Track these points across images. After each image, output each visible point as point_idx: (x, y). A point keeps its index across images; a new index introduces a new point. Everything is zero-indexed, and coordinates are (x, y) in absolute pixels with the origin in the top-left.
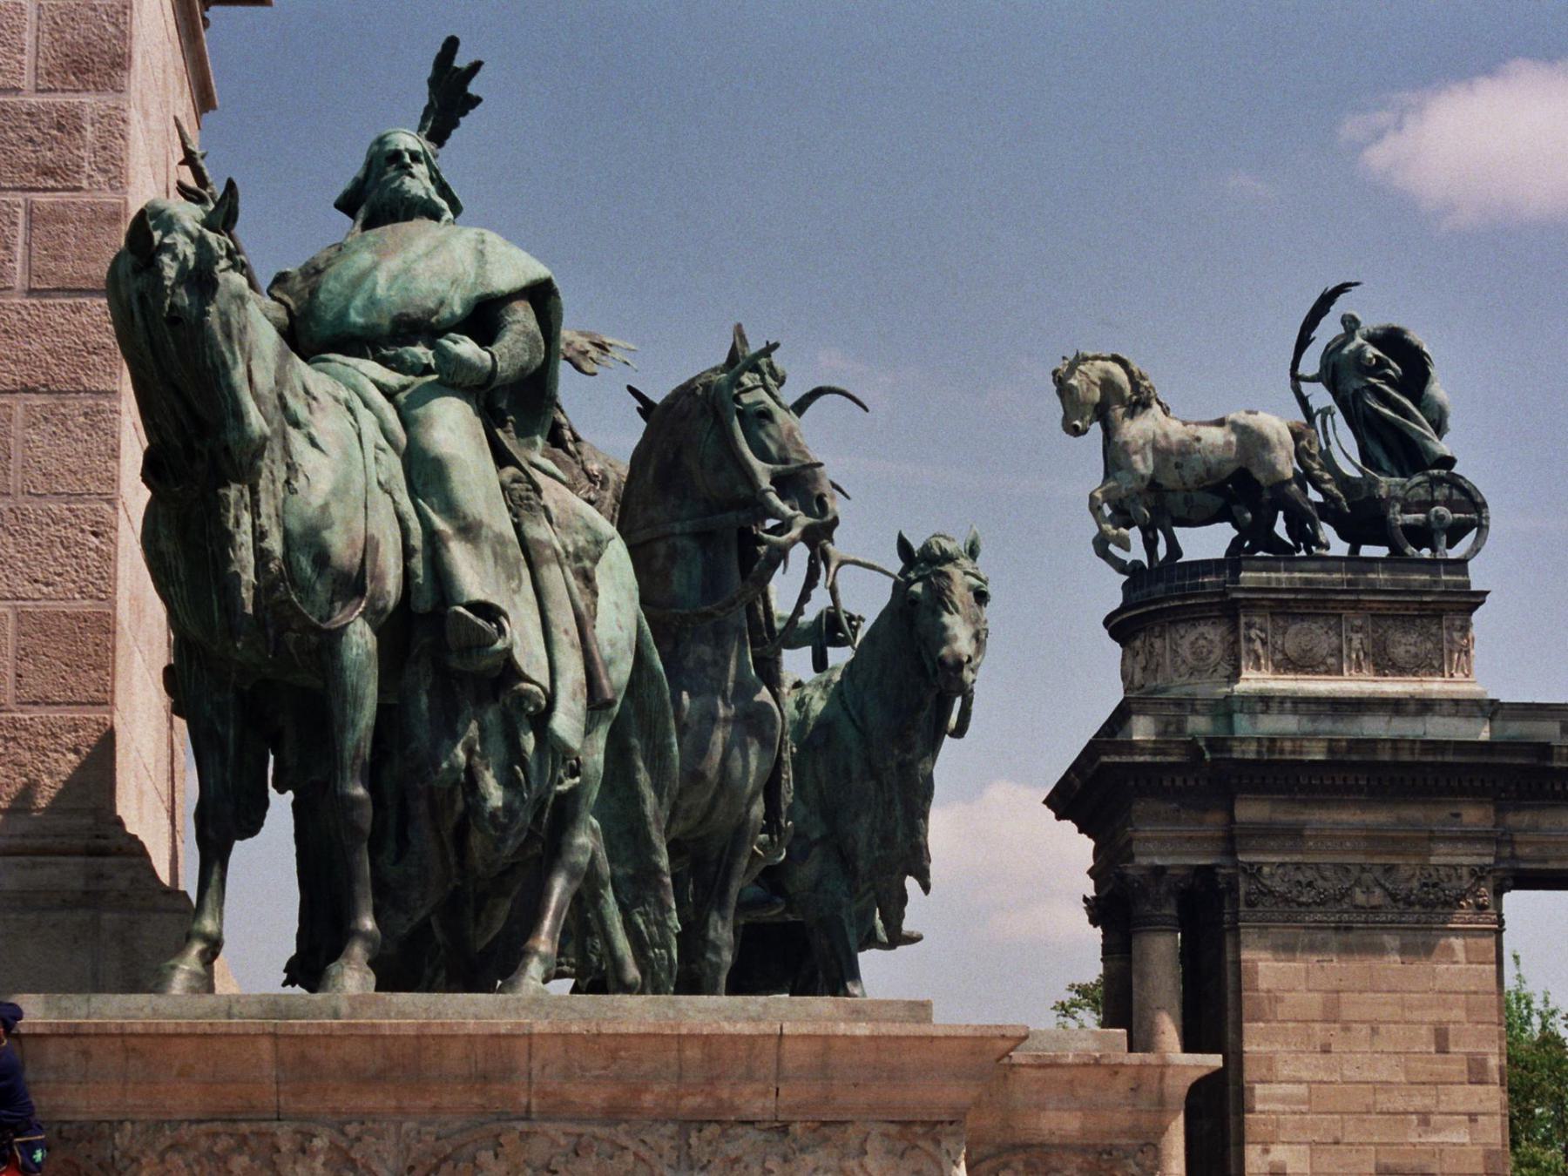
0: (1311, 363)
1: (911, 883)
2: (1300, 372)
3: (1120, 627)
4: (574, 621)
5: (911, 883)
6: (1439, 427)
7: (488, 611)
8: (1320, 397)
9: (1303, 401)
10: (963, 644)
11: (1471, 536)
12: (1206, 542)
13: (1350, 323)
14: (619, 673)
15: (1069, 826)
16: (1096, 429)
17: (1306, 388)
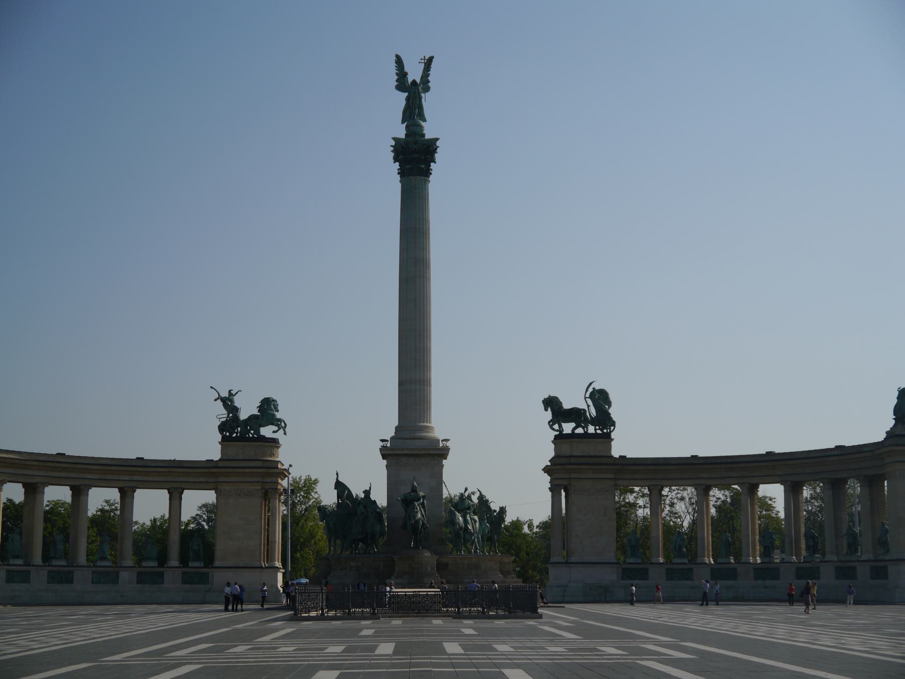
0: (588, 395)
3: (553, 442)
6: (610, 406)
8: (589, 401)
12: (568, 427)
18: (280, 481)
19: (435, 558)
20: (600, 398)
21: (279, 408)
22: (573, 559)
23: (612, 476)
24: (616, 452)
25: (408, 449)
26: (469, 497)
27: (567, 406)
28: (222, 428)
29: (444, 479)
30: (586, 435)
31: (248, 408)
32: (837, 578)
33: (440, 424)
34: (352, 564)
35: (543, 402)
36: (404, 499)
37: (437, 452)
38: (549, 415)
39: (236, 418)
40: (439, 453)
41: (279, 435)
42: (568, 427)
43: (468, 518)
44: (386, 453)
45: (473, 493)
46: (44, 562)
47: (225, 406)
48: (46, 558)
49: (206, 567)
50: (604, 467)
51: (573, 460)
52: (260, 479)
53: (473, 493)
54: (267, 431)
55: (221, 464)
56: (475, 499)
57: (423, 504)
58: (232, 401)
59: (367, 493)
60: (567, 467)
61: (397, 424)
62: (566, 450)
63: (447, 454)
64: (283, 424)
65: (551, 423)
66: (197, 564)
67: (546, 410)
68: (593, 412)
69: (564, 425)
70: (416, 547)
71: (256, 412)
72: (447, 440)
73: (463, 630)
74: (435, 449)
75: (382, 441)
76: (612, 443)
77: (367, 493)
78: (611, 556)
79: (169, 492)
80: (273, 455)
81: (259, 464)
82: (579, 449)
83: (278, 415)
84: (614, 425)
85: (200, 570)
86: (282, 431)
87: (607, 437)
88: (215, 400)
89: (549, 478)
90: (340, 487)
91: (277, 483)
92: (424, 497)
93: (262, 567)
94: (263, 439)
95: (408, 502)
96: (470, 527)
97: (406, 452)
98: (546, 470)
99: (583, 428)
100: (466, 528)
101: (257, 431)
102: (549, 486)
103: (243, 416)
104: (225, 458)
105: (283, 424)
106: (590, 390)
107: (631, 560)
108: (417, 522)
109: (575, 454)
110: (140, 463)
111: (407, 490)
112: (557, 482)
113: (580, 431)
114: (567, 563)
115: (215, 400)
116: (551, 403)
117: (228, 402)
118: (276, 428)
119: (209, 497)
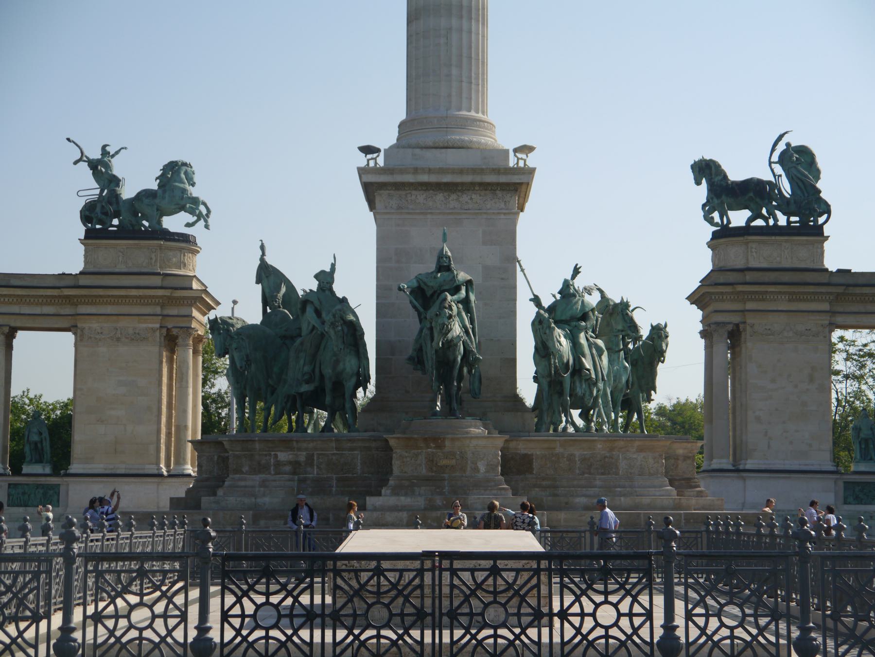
0: (775, 158)
1: (653, 392)
2: (772, 160)
3: (710, 245)
4: (599, 362)
5: (653, 392)
6: (818, 178)
7: (588, 370)
8: (778, 169)
9: (772, 170)
10: (664, 348)
11: (826, 216)
12: (739, 218)
13: (788, 145)
14: (605, 373)
15: (694, 307)
16: (704, 181)
17: (773, 165)
18: (195, 313)
19: (499, 441)
20: (799, 162)
21: (196, 179)
22: (750, 464)
23: (825, 306)
24: (833, 261)
25: (430, 171)
27: (736, 173)
28: (88, 214)
29: (520, 254)
30: (776, 230)
31: (136, 178)
33: (508, 115)
34: (283, 456)
35: (693, 167)
36: (422, 294)
37: (503, 179)
38: (702, 192)
40: (505, 186)
41: (197, 231)
42: (739, 218)
43: (583, 340)
44: (374, 189)
47: (97, 174)
49: (56, 473)
50: (811, 289)
51: (749, 276)
52: (158, 310)
54: (174, 223)
55: (83, 281)
57: (466, 302)
58: (107, 166)
59: (325, 279)
60: (740, 288)
61: (403, 116)
62: (737, 255)
63: (528, 185)
64: (202, 208)
65: (708, 208)
66: (37, 469)
67: (698, 183)
68: (786, 187)
69: (730, 213)
70: (450, 412)
71: (154, 186)
72: (527, 149)
74: (497, 171)
75: (367, 150)
76: (826, 244)
77: (325, 279)
78: (823, 459)
80: (182, 265)
81: (156, 281)
82: (763, 255)
83: (194, 192)
84: (829, 212)
85: (43, 480)
86: (202, 223)
87: (818, 231)
88: (76, 163)
89: (698, 314)
90: (268, 276)
91: (190, 317)
92: (469, 284)
93: (161, 475)
95: (427, 296)
96: (588, 364)
97: (424, 178)
98: (697, 299)
99: (766, 220)
101: (159, 223)
102: (700, 327)
103: (128, 192)
104: (92, 270)
105: (204, 212)
106: (781, 147)
107: (862, 467)
108: (450, 345)
109: (754, 264)
112: (720, 318)
113: (759, 222)
114: (738, 471)
115: (76, 163)
116: (706, 170)
117: (100, 168)
118: (191, 219)
119: (62, 344)
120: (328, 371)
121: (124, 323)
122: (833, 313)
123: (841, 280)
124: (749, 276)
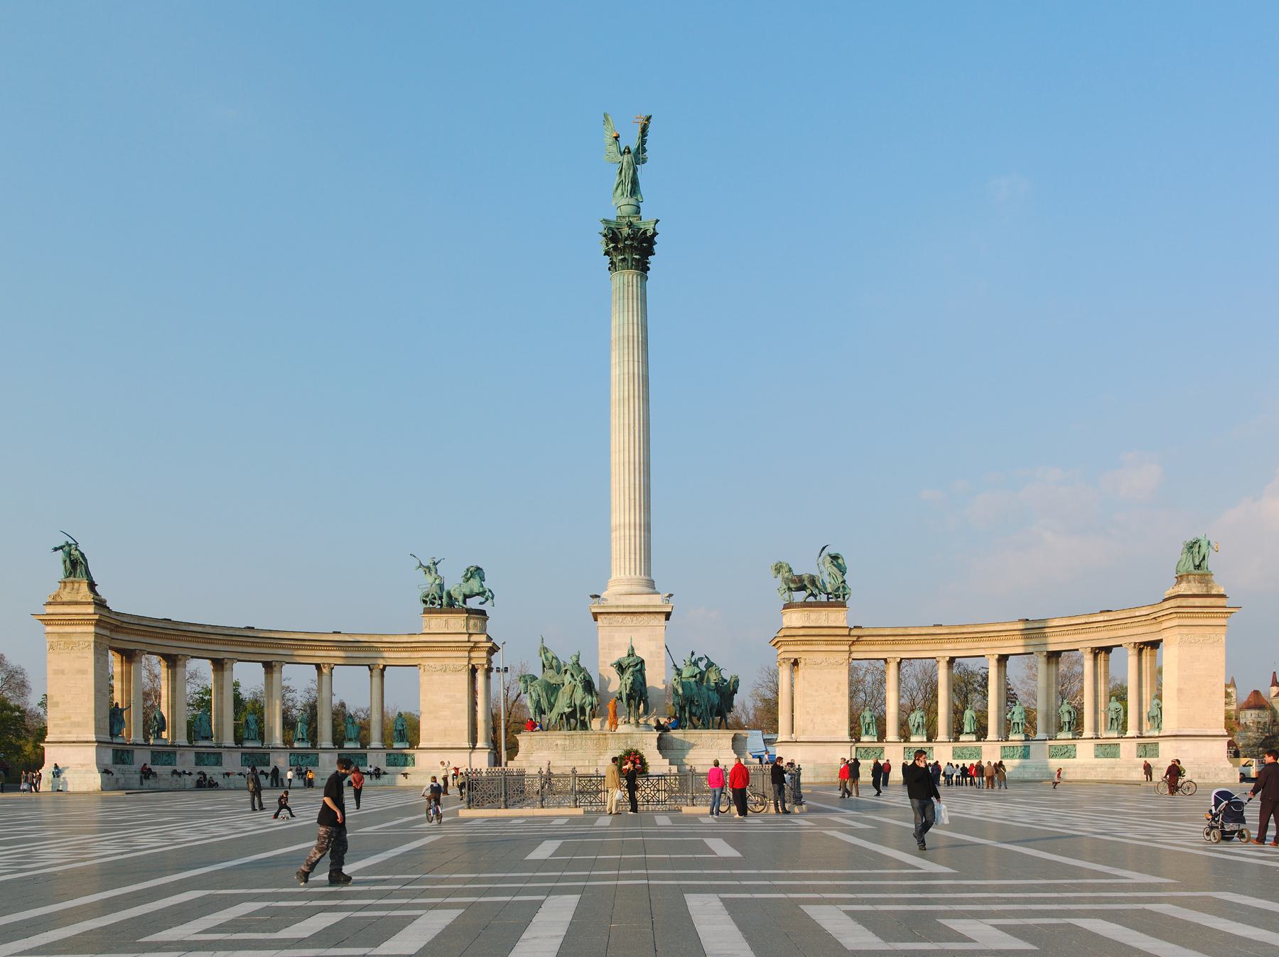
12: (800, 596)
26: (695, 664)
32: (1096, 756)
39: (441, 587)
45: (701, 659)
46: (190, 742)
48: (238, 740)
51: (802, 632)
53: (701, 659)
56: (702, 665)
73: (710, 842)
78: (844, 734)
79: (371, 670)
81: (465, 638)
83: (486, 585)
94: (469, 611)
99: (815, 596)
100: (692, 702)
101: (465, 602)
110: (337, 638)
111: (621, 654)
120: (578, 703)
121: (447, 662)
122: (851, 652)
123: (853, 633)
124: (802, 632)
